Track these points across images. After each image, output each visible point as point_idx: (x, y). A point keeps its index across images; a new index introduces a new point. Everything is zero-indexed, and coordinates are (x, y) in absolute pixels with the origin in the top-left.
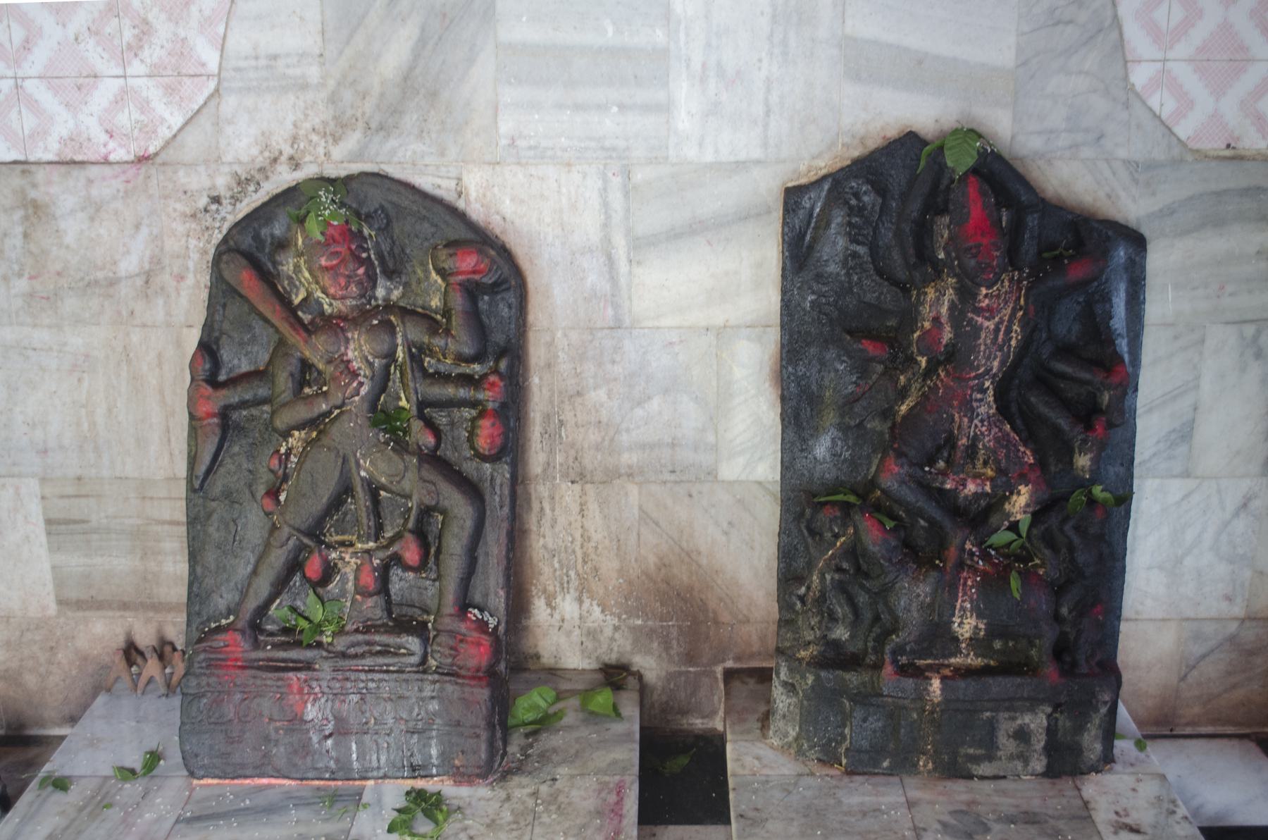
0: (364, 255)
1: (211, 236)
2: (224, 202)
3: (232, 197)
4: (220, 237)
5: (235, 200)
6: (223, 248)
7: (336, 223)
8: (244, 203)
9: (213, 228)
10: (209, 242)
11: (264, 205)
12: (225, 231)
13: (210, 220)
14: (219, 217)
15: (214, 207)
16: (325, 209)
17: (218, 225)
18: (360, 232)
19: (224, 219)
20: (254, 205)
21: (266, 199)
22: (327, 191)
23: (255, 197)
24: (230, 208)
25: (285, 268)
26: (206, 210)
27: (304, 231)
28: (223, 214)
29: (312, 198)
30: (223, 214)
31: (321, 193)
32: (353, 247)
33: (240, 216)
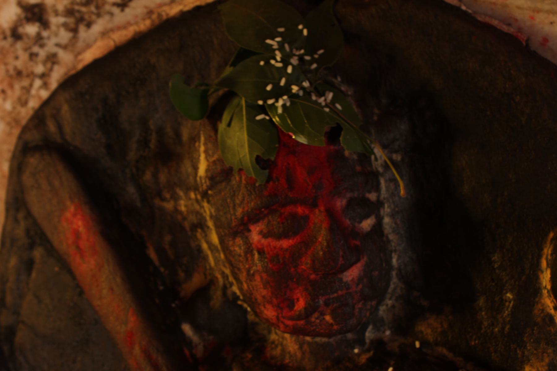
0: (367, 224)
1: (27, 90)
2: (55, 21)
3: (69, 12)
4: (45, 94)
5: (77, 20)
6: (34, 137)
7: (302, 140)
8: (97, 28)
9: (32, 75)
10: (24, 103)
11: (138, 42)
12: (54, 84)
13: (24, 56)
14: (42, 53)
15: (31, 29)
16: (277, 93)
17: (40, 69)
18: (365, 157)
19: (52, 59)
20: (120, 37)
21: (145, 25)
22: (292, 37)
23: (120, 17)
24: (65, 36)
25: (169, 206)
26: (16, 34)
27: (215, 141)
28: (50, 47)
29: (243, 55)
30: (50, 47)
31: (273, 43)
32: (340, 203)
33: (88, 57)
